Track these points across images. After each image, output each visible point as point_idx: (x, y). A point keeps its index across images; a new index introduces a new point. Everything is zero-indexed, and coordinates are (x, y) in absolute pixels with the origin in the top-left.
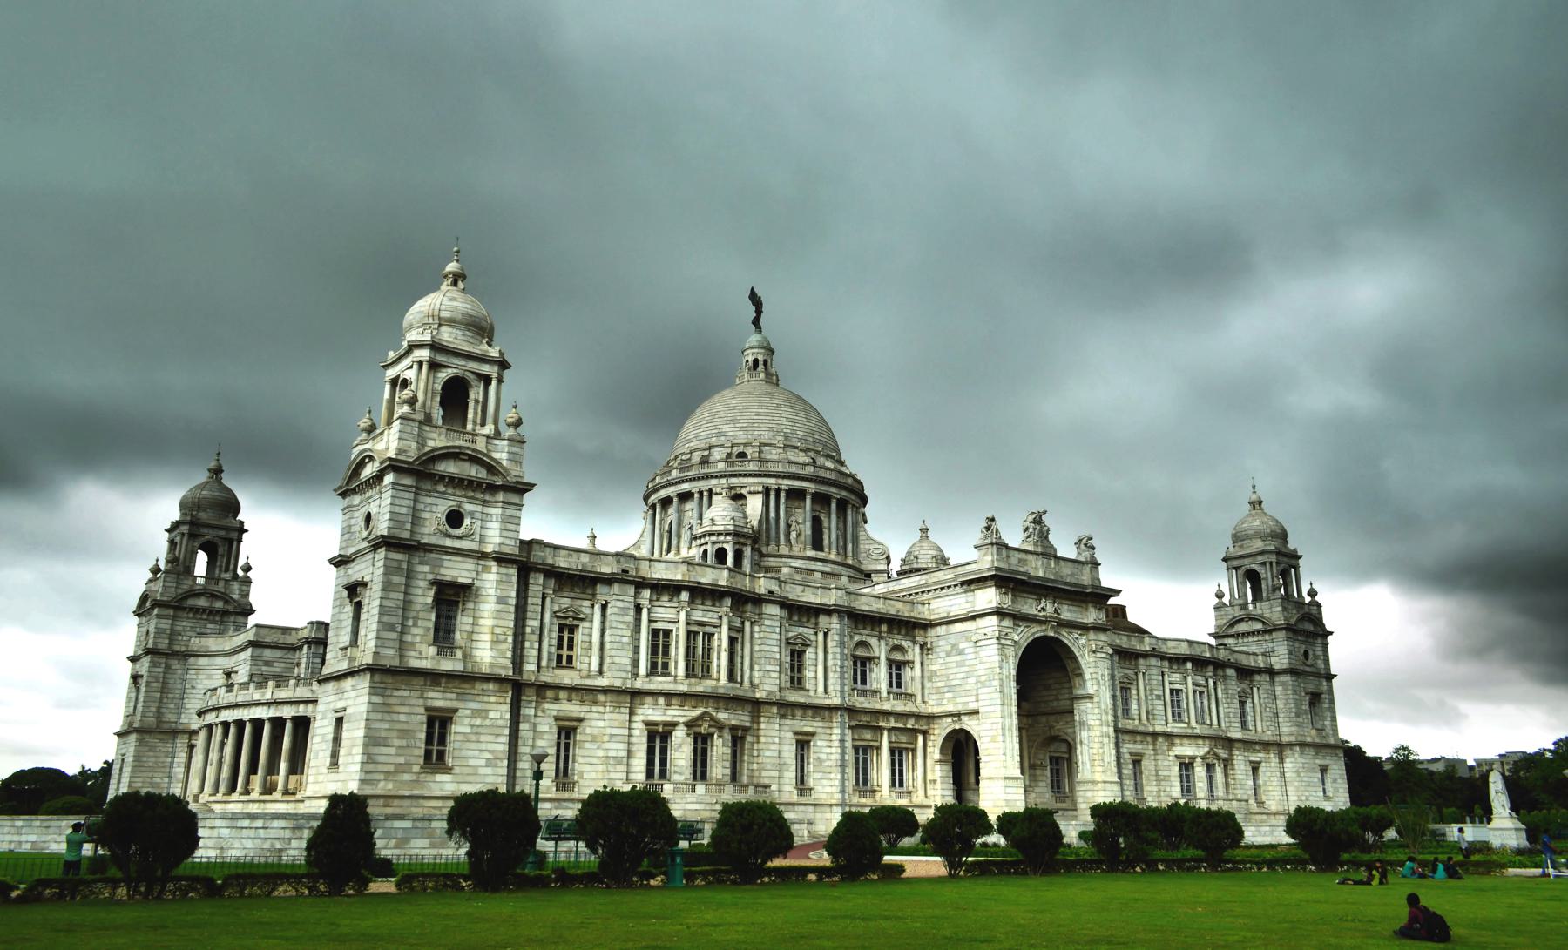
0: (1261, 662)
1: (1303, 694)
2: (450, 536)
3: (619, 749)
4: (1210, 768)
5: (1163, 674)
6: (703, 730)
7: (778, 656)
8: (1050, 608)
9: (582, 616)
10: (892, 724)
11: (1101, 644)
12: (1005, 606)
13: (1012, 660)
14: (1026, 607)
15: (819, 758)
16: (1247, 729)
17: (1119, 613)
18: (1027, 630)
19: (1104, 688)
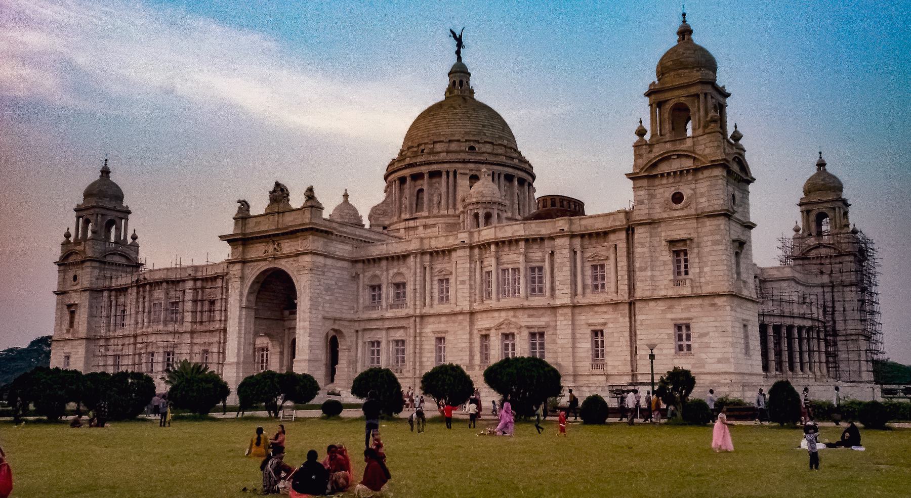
1: (664, 243)
2: (73, 286)
8: (271, 250)
11: (304, 264)
13: (238, 292)
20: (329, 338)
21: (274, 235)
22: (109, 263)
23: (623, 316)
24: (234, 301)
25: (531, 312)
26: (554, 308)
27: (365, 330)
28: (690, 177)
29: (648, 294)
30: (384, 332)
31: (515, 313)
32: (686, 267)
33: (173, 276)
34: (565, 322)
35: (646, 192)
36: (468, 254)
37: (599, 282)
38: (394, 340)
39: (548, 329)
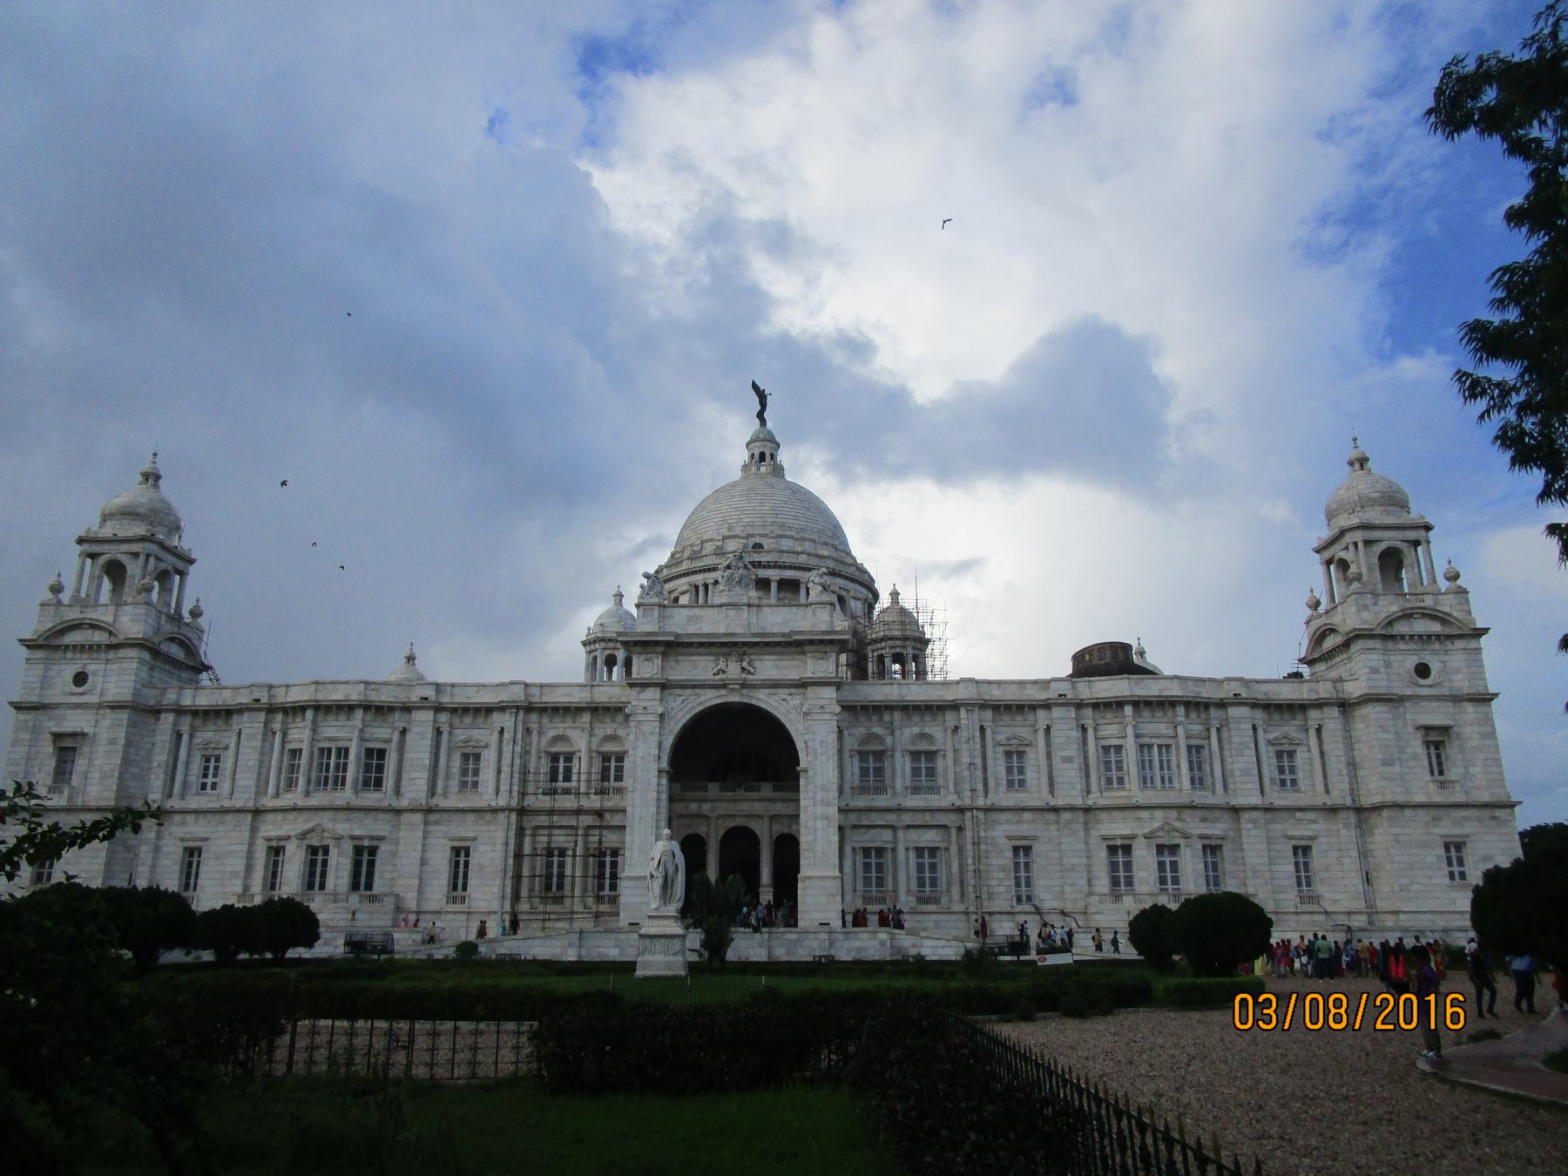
0: (1324, 690)
1: (1410, 729)
3: (239, 865)
4: (1167, 849)
5: (1084, 729)
6: (315, 843)
7: (427, 762)
8: (733, 670)
9: (222, 746)
10: (587, 820)
11: (821, 702)
12: (647, 676)
14: (694, 672)
15: (480, 864)
18: (692, 698)
19: (824, 758)
20: (775, 837)
23: (1347, 826)
26: (1235, 810)
27: (855, 827)
28: (1437, 646)
29: (1401, 799)
31: (1179, 814)
32: (1440, 764)
33: (384, 697)
34: (1254, 832)
35: (1381, 657)
36: (1073, 715)
38: (916, 848)
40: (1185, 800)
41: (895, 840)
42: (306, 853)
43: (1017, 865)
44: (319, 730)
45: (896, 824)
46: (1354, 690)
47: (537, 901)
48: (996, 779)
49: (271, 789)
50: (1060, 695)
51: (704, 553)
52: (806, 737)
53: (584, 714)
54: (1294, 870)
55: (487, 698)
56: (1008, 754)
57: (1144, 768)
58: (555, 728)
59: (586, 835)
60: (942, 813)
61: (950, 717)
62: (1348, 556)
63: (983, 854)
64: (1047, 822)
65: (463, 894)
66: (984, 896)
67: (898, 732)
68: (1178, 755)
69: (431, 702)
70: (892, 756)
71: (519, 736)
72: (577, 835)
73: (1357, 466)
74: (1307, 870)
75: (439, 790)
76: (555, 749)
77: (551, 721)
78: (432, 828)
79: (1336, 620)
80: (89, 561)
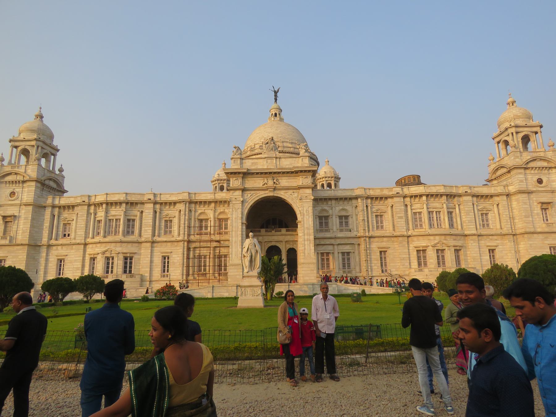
0: (500, 189)
1: (535, 204)
3: (79, 265)
5: (406, 205)
6: (108, 255)
7: (151, 223)
10: (215, 244)
15: (173, 262)
16: (490, 228)
17: (416, 179)
18: (254, 195)
20: (287, 249)
21: (275, 173)
22: (47, 185)
24: (235, 218)
25: (454, 237)
26: (466, 236)
28: (546, 171)
29: (532, 230)
30: (336, 247)
34: (474, 244)
35: (524, 176)
36: (402, 200)
37: (485, 223)
38: (342, 252)
39: (463, 248)
40: (448, 232)
41: (334, 250)
42: (105, 260)
43: (381, 258)
44: (109, 212)
45: (334, 243)
46: (512, 189)
47: (196, 276)
48: (372, 225)
49: (90, 236)
50: (397, 193)
51: (255, 148)
52: (300, 209)
53: (212, 204)
54: (489, 258)
55: (174, 198)
56: (377, 216)
57: (430, 220)
58: (201, 209)
59: (214, 250)
60: (351, 239)
61: (354, 201)
62: (509, 139)
63: (368, 254)
64: (393, 242)
65: (168, 273)
66: (369, 270)
67: (334, 208)
68: (444, 215)
69: (153, 200)
70: (332, 218)
71: (187, 213)
72: (210, 250)
73: (511, 105)
74: (494, 259)
75: (156, 234)
76: (201, 217)
77: (199, 207)
78: (155, 249)
79: (504, 162)
80: (15, 150)
